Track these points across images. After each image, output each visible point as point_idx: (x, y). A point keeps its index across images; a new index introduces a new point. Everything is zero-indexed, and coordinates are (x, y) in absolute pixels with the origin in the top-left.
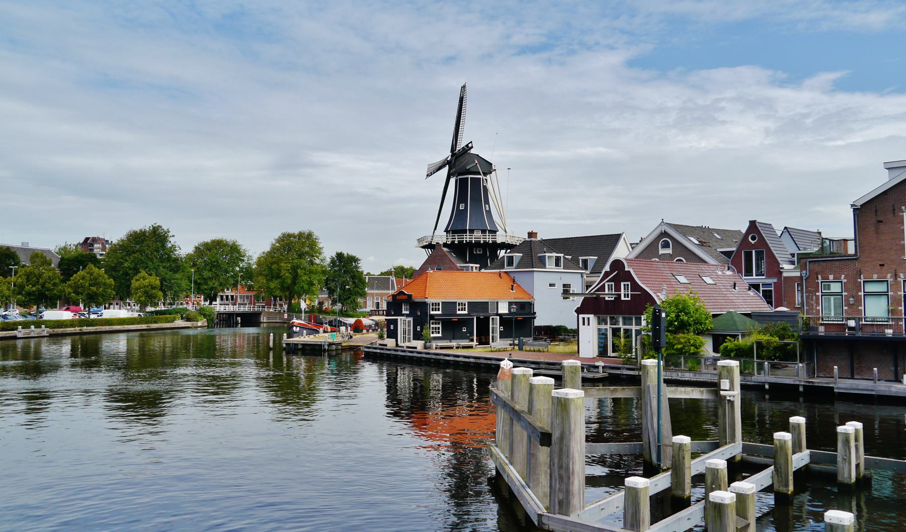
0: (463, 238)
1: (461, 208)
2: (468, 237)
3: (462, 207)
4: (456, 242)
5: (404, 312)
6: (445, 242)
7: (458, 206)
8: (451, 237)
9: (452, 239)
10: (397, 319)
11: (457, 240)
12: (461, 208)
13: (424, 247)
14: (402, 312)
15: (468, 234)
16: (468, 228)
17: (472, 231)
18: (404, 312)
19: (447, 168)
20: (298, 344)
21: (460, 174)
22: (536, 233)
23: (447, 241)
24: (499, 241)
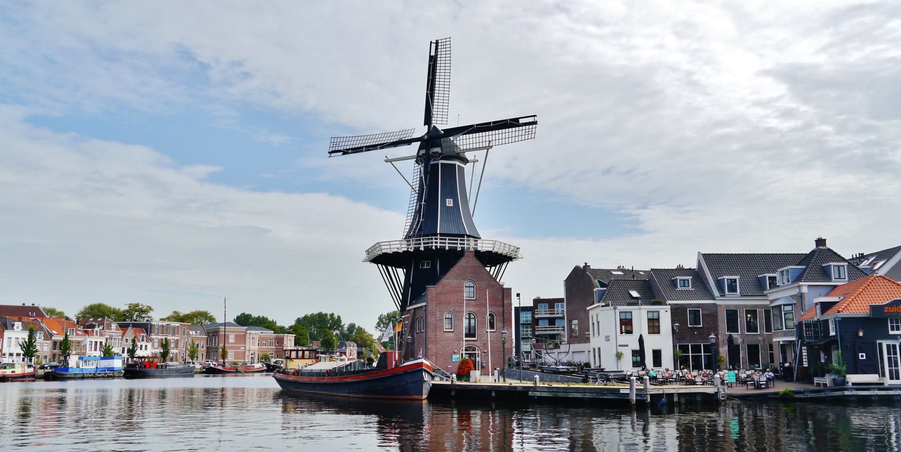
0: (457, 244)
1: (452, 205)
3: (450, 203)
6: (406, 249)
7: (443, 203)
8: (414, 242)
9: (415, 244)
11: (411, 246)
12: (447, 205)
14: (888, 332)
16: (438, 232)
18: (891, 332)
19: (419, 143)
20: (672, 394)
21: (443, 158)
22: (826, 240)
23: (408, 248)
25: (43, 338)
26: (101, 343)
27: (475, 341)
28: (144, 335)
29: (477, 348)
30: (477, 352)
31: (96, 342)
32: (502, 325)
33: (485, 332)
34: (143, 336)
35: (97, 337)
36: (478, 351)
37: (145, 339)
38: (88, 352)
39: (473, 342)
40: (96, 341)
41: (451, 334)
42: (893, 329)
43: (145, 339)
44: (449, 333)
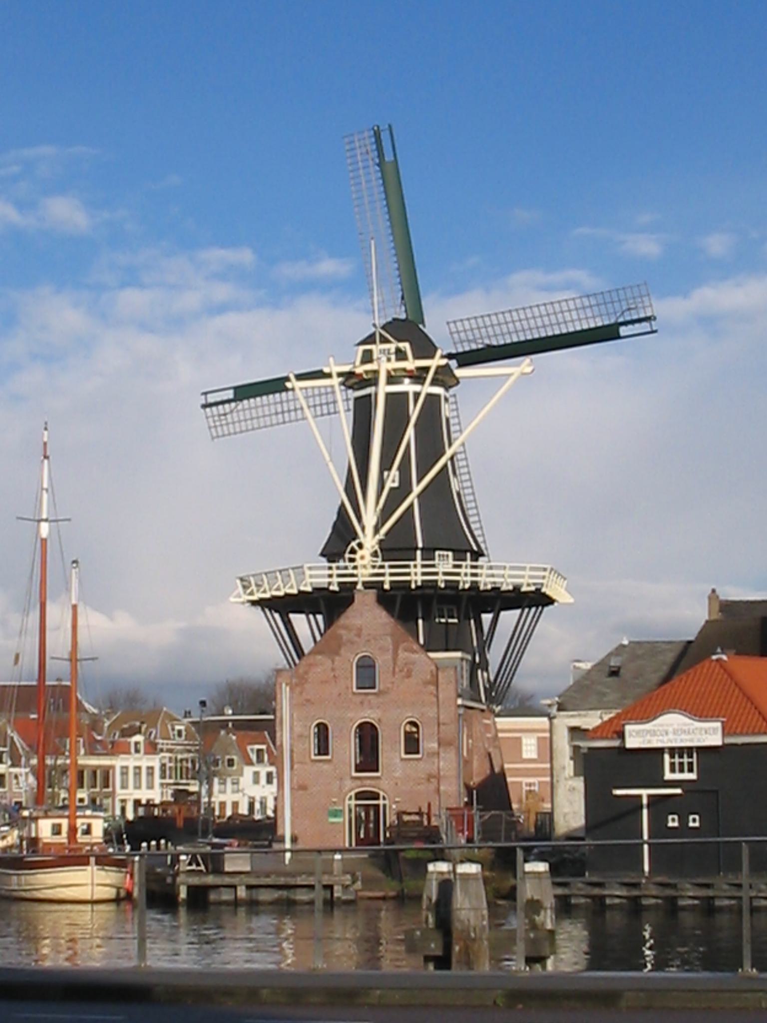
2: (420, 570)
4: (335, 588)
5: (668, 776)
10: (640, 797)
13: (254, 603)
14: (663, 775)
15: (419, 561)
17: (429, 553)
18: (668, 776)
24: (485, 582)
25: (9, 763)
26: (151, 770)
27: (378, 778)
28: (264, 747)
29: (382, 794)
30: (381, 802)
31: (138, 768)
32: (436, 745)
33: (398, 761)
34: (259, 752)
35: (137, 755)
36: (384, 798)
37: (266, 757)
38: (118, 790)
39: (373, 782)
40: (138, 764)
41: (326, 767)
42: (673, 770)
43: (266, 757)
44: (321, 764)
